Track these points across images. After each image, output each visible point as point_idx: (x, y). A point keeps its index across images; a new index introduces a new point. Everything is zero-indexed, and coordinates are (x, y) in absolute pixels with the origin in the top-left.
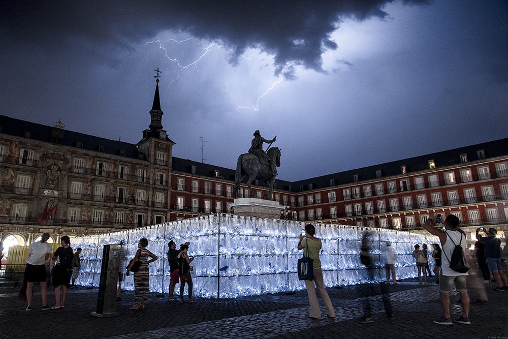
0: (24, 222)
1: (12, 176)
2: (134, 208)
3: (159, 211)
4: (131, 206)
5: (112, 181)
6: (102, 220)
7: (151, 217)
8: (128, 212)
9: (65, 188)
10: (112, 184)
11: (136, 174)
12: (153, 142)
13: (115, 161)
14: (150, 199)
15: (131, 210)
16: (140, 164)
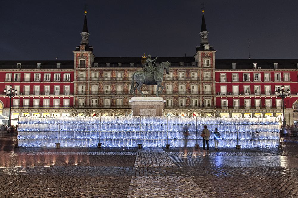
0: (97, 108)
1: (127, 86)
2: (191, 96)
3: (208, 97)
4: (188, 95)
5: (176, 82)
6: (172, 104)
7: (202, 101)
8: (187, 99)
9: (151, 89)
10: (176, 84)
11: (190, 76)
12: (200, 54)
13: (176, 70)
14: (201, 90)
15: (188, 98)
16: (192, 70)
